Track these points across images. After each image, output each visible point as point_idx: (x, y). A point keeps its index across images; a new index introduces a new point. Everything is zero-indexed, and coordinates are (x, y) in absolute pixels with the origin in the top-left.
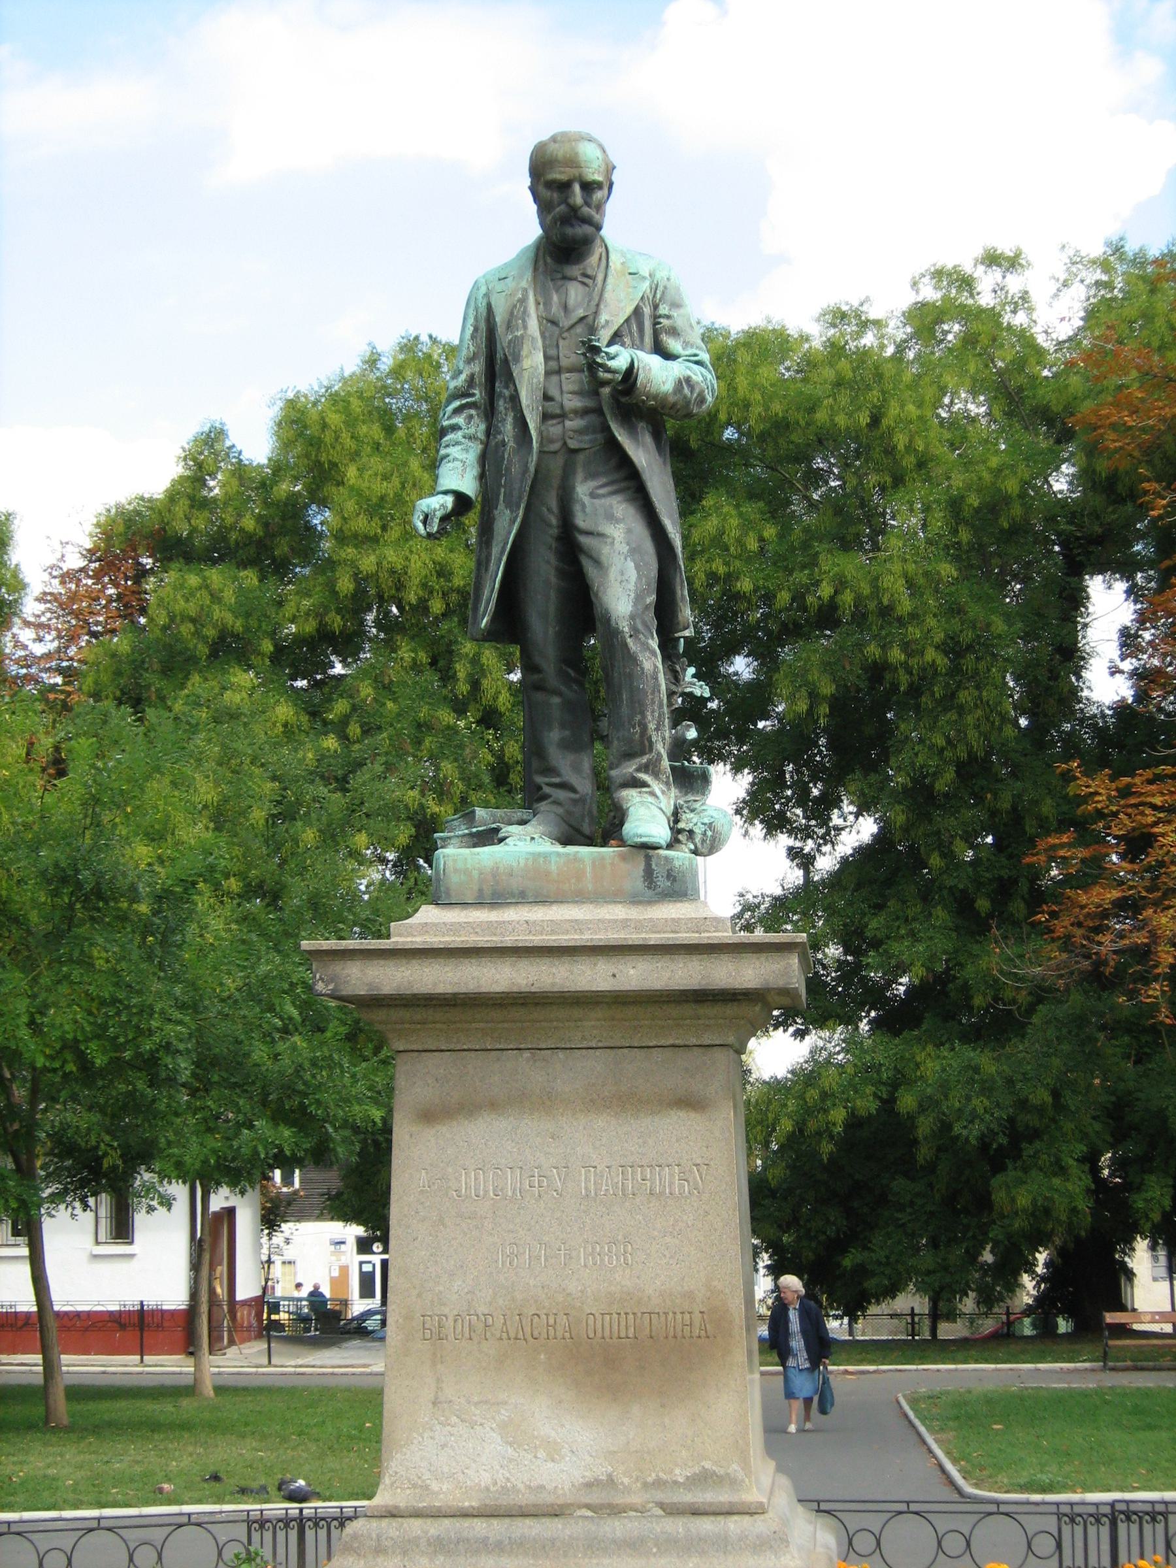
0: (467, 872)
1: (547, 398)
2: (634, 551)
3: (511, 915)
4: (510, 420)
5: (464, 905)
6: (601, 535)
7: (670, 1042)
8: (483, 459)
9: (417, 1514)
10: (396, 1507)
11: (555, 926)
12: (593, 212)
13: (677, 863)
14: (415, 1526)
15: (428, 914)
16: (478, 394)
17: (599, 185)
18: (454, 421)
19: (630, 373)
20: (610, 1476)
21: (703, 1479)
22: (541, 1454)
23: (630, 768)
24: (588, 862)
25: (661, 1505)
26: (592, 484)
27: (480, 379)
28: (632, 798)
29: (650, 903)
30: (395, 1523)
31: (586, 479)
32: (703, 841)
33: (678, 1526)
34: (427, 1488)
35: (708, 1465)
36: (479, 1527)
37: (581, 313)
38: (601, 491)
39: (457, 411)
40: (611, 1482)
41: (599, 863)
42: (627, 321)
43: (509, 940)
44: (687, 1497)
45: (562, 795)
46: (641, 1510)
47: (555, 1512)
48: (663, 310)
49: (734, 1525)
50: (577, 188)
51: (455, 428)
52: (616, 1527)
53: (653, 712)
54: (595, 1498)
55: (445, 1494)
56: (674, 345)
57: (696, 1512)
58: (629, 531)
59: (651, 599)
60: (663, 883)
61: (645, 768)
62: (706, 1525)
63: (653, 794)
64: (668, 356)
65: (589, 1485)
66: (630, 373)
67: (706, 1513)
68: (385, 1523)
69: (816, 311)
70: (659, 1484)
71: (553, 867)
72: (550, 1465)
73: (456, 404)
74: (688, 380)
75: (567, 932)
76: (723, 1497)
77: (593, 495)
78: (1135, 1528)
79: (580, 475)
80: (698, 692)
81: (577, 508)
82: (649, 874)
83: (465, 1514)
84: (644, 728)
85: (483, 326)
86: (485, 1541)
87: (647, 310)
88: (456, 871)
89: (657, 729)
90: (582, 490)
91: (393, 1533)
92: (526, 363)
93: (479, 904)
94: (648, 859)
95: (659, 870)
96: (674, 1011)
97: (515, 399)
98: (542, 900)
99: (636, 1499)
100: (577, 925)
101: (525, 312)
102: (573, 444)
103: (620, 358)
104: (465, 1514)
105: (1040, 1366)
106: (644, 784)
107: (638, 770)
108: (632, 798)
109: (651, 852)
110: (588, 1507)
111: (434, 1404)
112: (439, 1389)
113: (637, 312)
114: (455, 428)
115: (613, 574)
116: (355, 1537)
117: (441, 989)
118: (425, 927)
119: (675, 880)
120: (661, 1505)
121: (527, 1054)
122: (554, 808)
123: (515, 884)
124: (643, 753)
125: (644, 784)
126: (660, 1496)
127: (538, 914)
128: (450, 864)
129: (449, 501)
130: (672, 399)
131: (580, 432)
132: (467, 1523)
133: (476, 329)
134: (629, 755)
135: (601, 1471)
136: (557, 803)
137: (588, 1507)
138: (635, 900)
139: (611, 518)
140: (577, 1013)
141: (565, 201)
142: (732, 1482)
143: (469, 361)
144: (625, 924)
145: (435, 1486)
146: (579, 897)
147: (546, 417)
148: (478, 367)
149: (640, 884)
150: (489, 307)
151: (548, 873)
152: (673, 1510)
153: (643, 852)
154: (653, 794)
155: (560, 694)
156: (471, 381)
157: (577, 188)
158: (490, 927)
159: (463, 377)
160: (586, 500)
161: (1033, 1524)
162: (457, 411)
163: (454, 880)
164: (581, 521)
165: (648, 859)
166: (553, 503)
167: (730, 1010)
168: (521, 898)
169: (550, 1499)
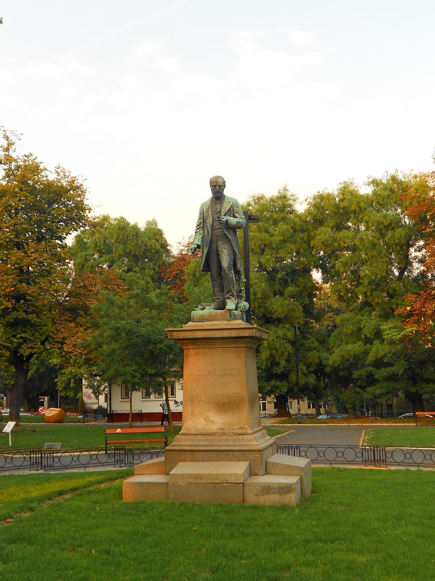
0: (197, 315)
1: (213, 226)
2: (229, 255)
3: (205, 323)
4: (206, 231)
7: (234, 346)
8: (202, 238)
9: (188, 434)
10: (184, 433)
12: (221, 191)
13: (235, 313)
14: (188, 437)
15: (190, 323)
17: (222, 186)
19: (227, 221)
21: (241, 428)
22: (211, 423)
24: (219, 313)
26: (221, 242)
28: (228, 301)
30: (184, 436)
31: (220, 241)
33: (235, 437)
34: (190, 430)
35: (241, 425)
37: (219, 210)
40: (224, 429)
41: (221, 313)
42: (228, 211)
45: (217, 300)
47: (213, 434)
48: (235, 208)
49: (245, 437)
50: (217, 186)
52: (224, 437)
55: (193, 431)
56: (237, 215)
58: (228, 251)
59: (232, 263)
60: (233, 317)
62: (240, 437)
63: (232, 300)
64: (235, 217)
65: (220, 429)
66: (227, 221)
67: (241, 435)
68: (182, 436)
69: (157, 220)
70: (233, 429)
71: (213, 314)
72: (212, 425)
73: (198, 227)
74: (239, 222)
75: (215, 326)
76: (244, 431)
79: (219, 240)
80: (244, 280)
81: (219, 246)
82: (230, 315)
84: (230, 288)
85: (202, 213)
87: (232, 209)
88: (195, 315)
90: (220, 243)
91: (184, 438)
92: (208, 220)
93: (199, 321)
96: (233, 340)
97: (207, 226)
103: (225, 219)
106: (231, 298)
107: (229, 296)
108: (228, 301)
111: (191, 414)
112: (192, 411)
113: (230, 209)
115: (225, 259)
116: (177, 438)
118: (189, 326)
119: (235, 316)
121: (208, 349)
122: (216, 303)
123: (206, 317)
125: (231, 298)
127: (210, 323)
128: (194, 314)
129: (196, 245)
130: (236, 226)
134: (228, 293)
135: (222, 426)
136: (217, 302)
137: (219, 433)
138: (229, 320)
139: (225, 248)
140: (216, 341)
141: (215, 189)
144: (225, 324)
145: (192, 429)
146: (217, 320)
147: (212, 230)
148: (201, 220)
149: (228, 317)
151: (212, 315)
153: (229, 311)
154: (232, 300)
155: (217, 282)
157: (217, 186)
158: (201, 326)
160: (221, 245)
163: (195, 317)
164: (219, 249)
165: (230, 312)
166: (215, 246)
167: (244, 340)
168: (207, 320)
169: (211, 431)
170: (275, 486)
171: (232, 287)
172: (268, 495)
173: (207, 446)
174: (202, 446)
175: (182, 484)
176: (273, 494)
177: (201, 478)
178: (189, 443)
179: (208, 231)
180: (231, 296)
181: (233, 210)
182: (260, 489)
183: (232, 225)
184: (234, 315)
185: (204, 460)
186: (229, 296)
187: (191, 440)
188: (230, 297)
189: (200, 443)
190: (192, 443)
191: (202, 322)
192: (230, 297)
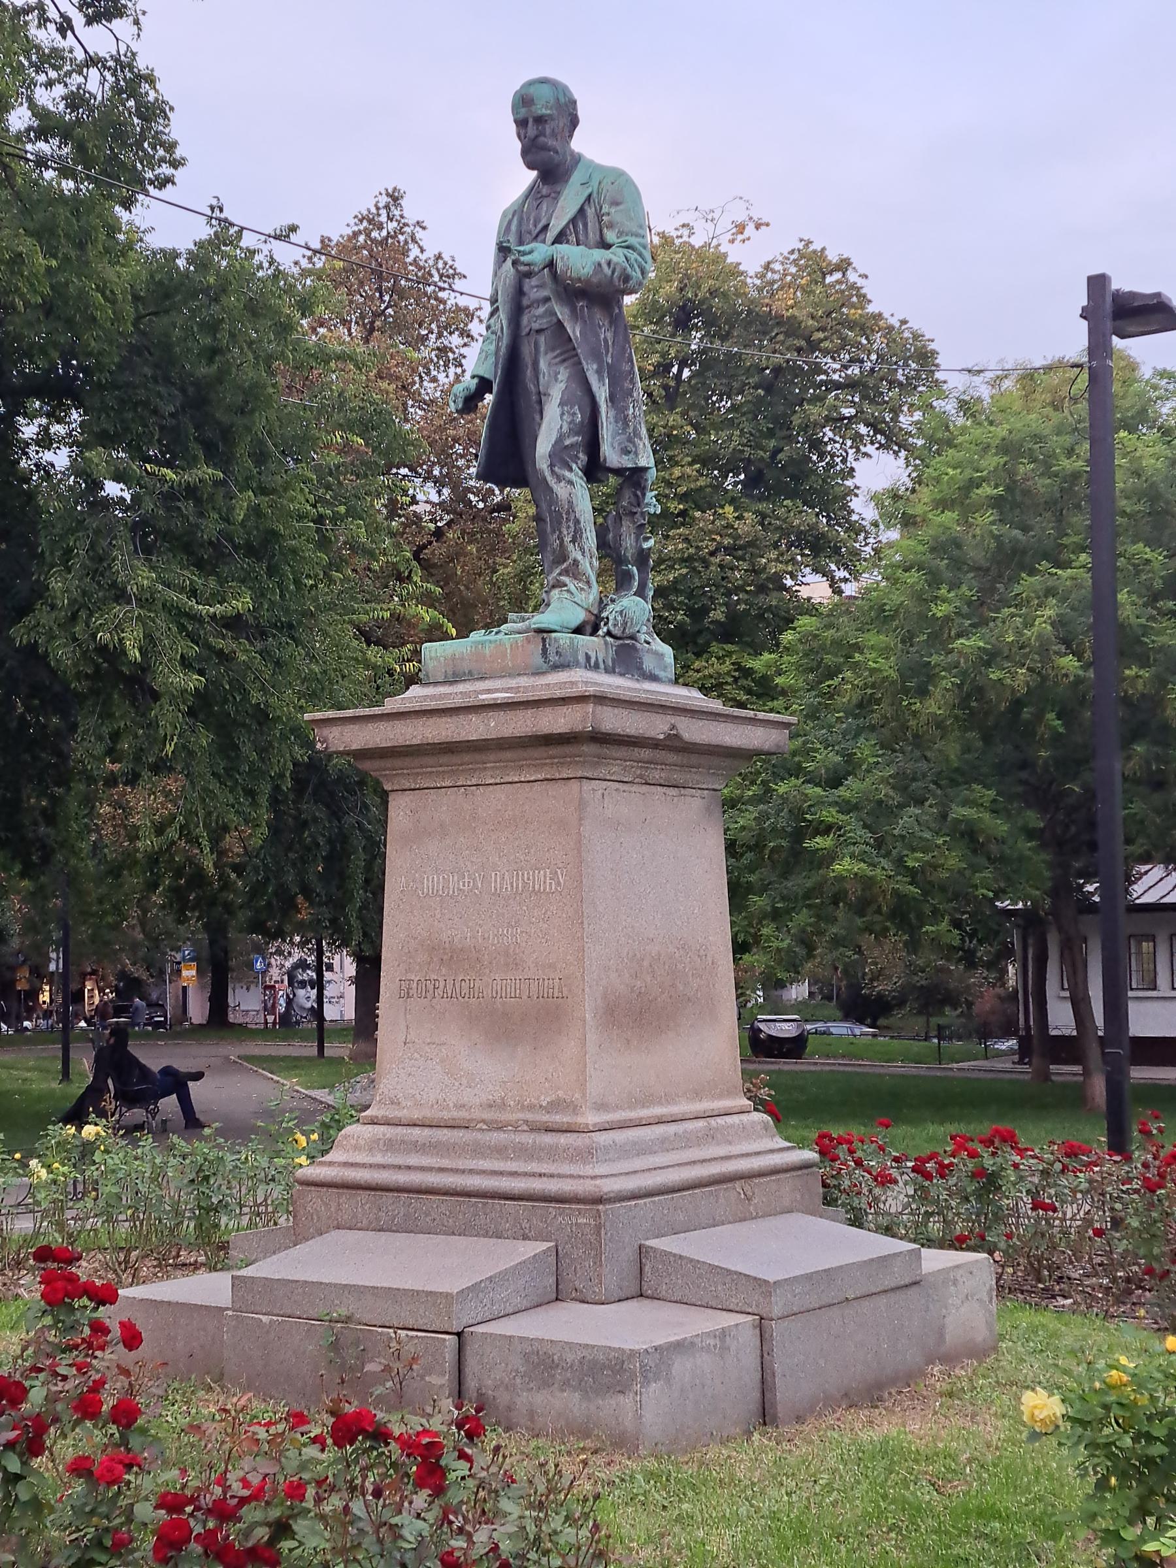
3: (460, 688)
5: (436, 683)
15: (415, 691)
19: (551, 264)
21: (555, 1106)
25: (526, 1122)
32: (615, 625)
33: (528, 1139)
35: (560, 1093)
38: (558, 360)
40: (503, 1106)
49: (563, 1140)
53: (569, 527)
54: (488, 1115)
60: (553, 658)
61: (566, 572)
62: (548, 1139)
70: (531, 1108)
82: (545, 651)
87: (590, 212)
89: (573, 541)
94: (544, 640)
95: (551, 650)
107: (560, 574)
109: (545, 635)
116: (346, 1137)
121: (462, 789)
126: (530, 1116)
132: (410, 1130)
137: (483, 1121)
142: (575, 1109)
149: (540, 660)
152: (535, 1128)
153: (541, 635)
154: (568, 591)
165: (544, 640)
170: (570, 1357)
171: (567, 539)
172: (545, 1392)
180: (568, 575)
181: (599, 216)
182: (517, 1362)
183: (579, 280)
186: (560, 574)
188: (563, 578)
189: (413, 1160)
190: (390, 1159)
191: (451, 683)
192: (563, 578)
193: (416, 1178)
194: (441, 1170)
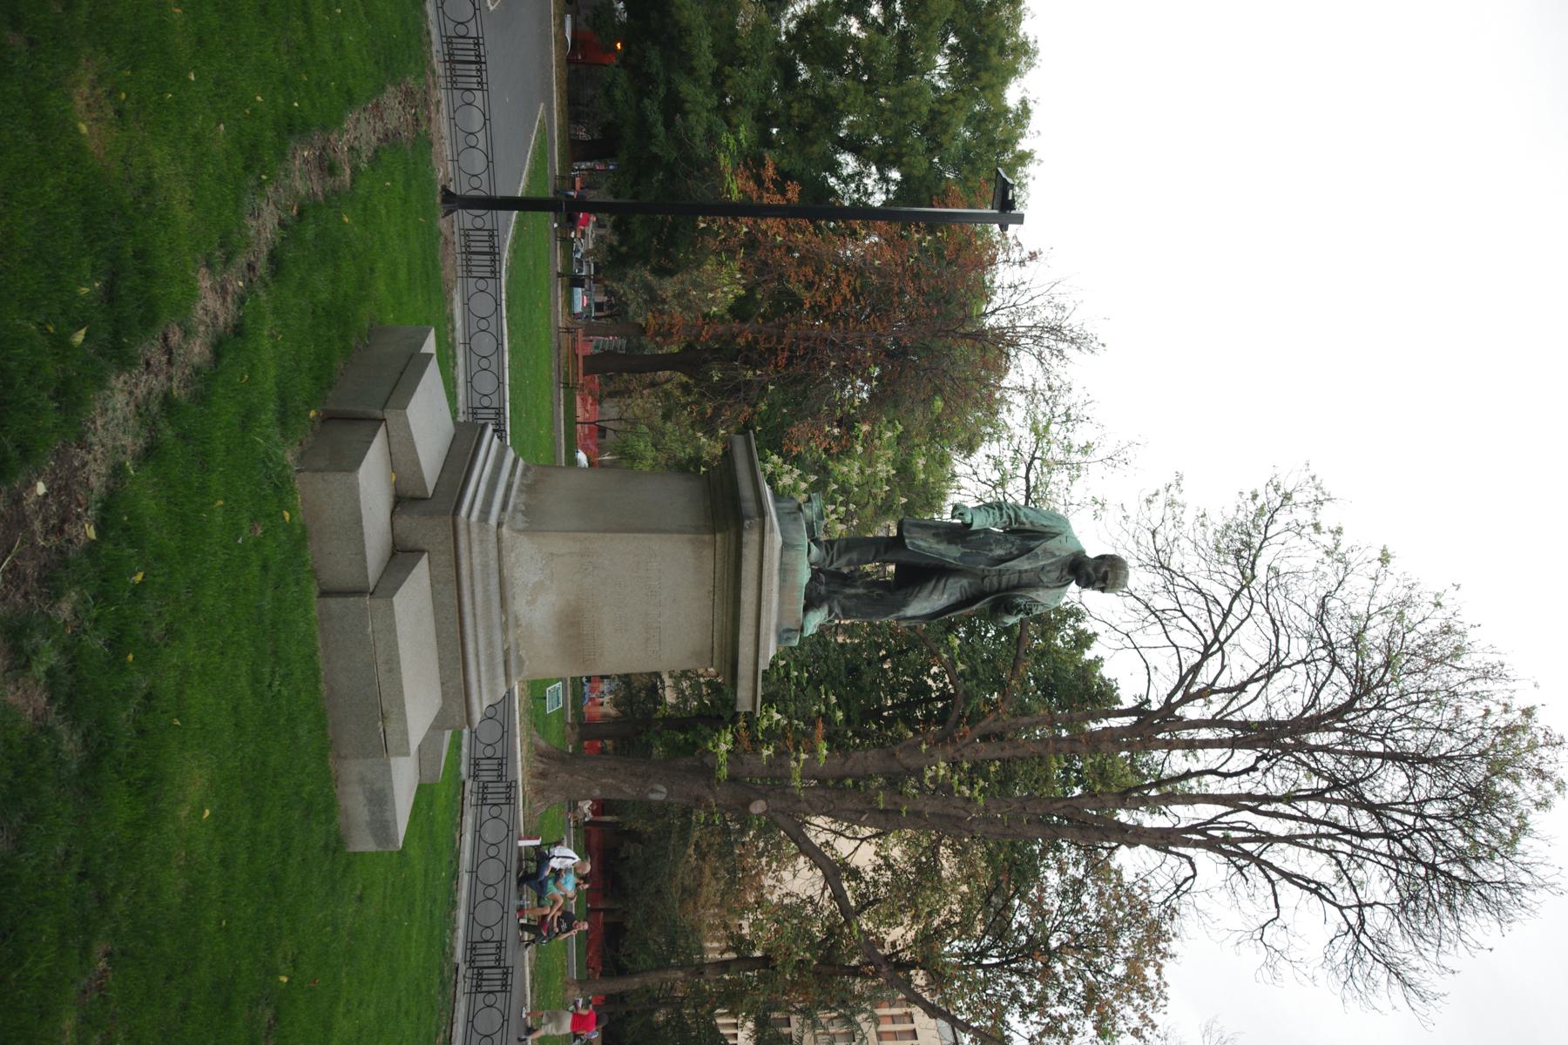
6: (943, 593)
9: (499, 551)
11: (771, 575)
14: (493, 554)
16: (1015, 526)
18: (1005, 516)
20: (520, 625)
21: (520, 661)
22: (529, 598)
23: (837, 610)
25: (508, 649)
27: (1022, 527)
29: (777, 631)
33: (500, 659)
35: (527, 663)
36: (494, 581)
39: (1009, 516)
40: (518, 626)
43: (764, 614)
44: (512, 658)
45: (828, 562)
46: (505, 641)
51: (1001, 515)
55: (510, 559)
57: (506, 663)
60: (785, 636)
62: (500, 670)
65: (516, 617)
70: (518, 645)
76: (513, 670)
77: (961, 586)
78: (488, 263)
79: (971, 581)
81: (957, 579)
82: (790, 630)
83: (500, 571)
84: (854, 617)
86: (488, 585)
90: (965, 582)
91: (490, 546)
92: (1026, 562)
93: (781, 563)
95: (790, 635)
98: (781, 588)
99: (511, 638)
100: (770, 602)
101: (1049, 558)
102: (986, 580)
104: (500, 571)
105: (562, 422)
110: (507, 620)
114: (1001, 515)
115: (926, 604)
117: (743, 573)
120: (508, 649)
124: (843, 614)
126: (513, 647)
131: (991, 583)
133: (1045, 526)
135: (523, 622)
136: (824, 560)
137: (507, 620)
138: (779, 625)
141: (1097, 579)
142: (520, 673)
143: (1032, 523)
145: (513, 555)
146: (781, 603)
148: (1028, 526)
149: (786, 625)
150: (1058, 534)
152: (506, 653)
156: (1023, 524)
157: (1103, 585)
159: (1025, 520)
160: (959, 584)
161: (495, 398)
162: (1009, 516)
164: (951, 581)
168: (783, 580)
173: (474, 608)
174: (473, 604)
175: (370, 629)
176: (369, 810)
177: (390, 671)
178: (477, 561)
179: (1001, 560)
184: (788, 639)
185: (438, 607)
187: (485, 566)
189: (479, 589)
190: (477, 568)
193: (467, 608)
194: (475, 615)
